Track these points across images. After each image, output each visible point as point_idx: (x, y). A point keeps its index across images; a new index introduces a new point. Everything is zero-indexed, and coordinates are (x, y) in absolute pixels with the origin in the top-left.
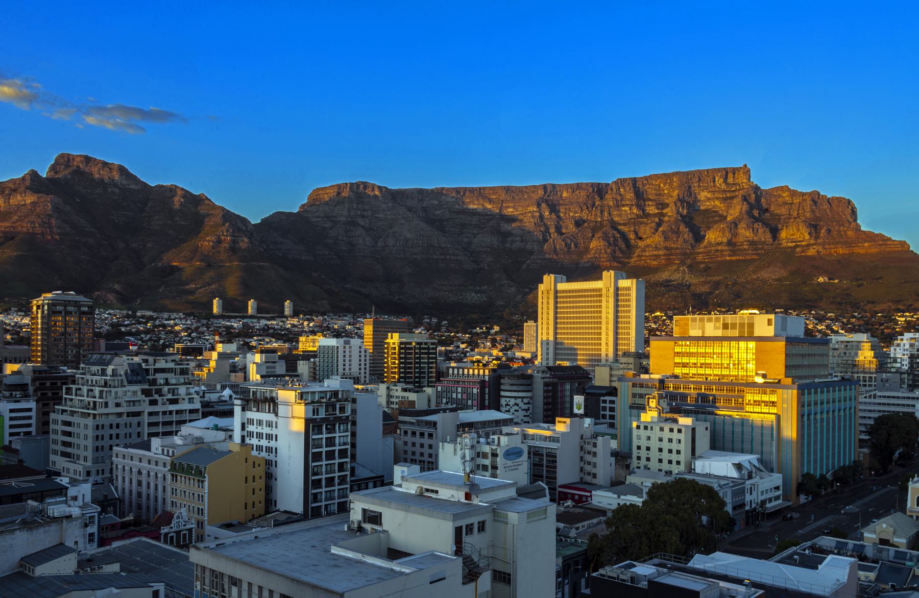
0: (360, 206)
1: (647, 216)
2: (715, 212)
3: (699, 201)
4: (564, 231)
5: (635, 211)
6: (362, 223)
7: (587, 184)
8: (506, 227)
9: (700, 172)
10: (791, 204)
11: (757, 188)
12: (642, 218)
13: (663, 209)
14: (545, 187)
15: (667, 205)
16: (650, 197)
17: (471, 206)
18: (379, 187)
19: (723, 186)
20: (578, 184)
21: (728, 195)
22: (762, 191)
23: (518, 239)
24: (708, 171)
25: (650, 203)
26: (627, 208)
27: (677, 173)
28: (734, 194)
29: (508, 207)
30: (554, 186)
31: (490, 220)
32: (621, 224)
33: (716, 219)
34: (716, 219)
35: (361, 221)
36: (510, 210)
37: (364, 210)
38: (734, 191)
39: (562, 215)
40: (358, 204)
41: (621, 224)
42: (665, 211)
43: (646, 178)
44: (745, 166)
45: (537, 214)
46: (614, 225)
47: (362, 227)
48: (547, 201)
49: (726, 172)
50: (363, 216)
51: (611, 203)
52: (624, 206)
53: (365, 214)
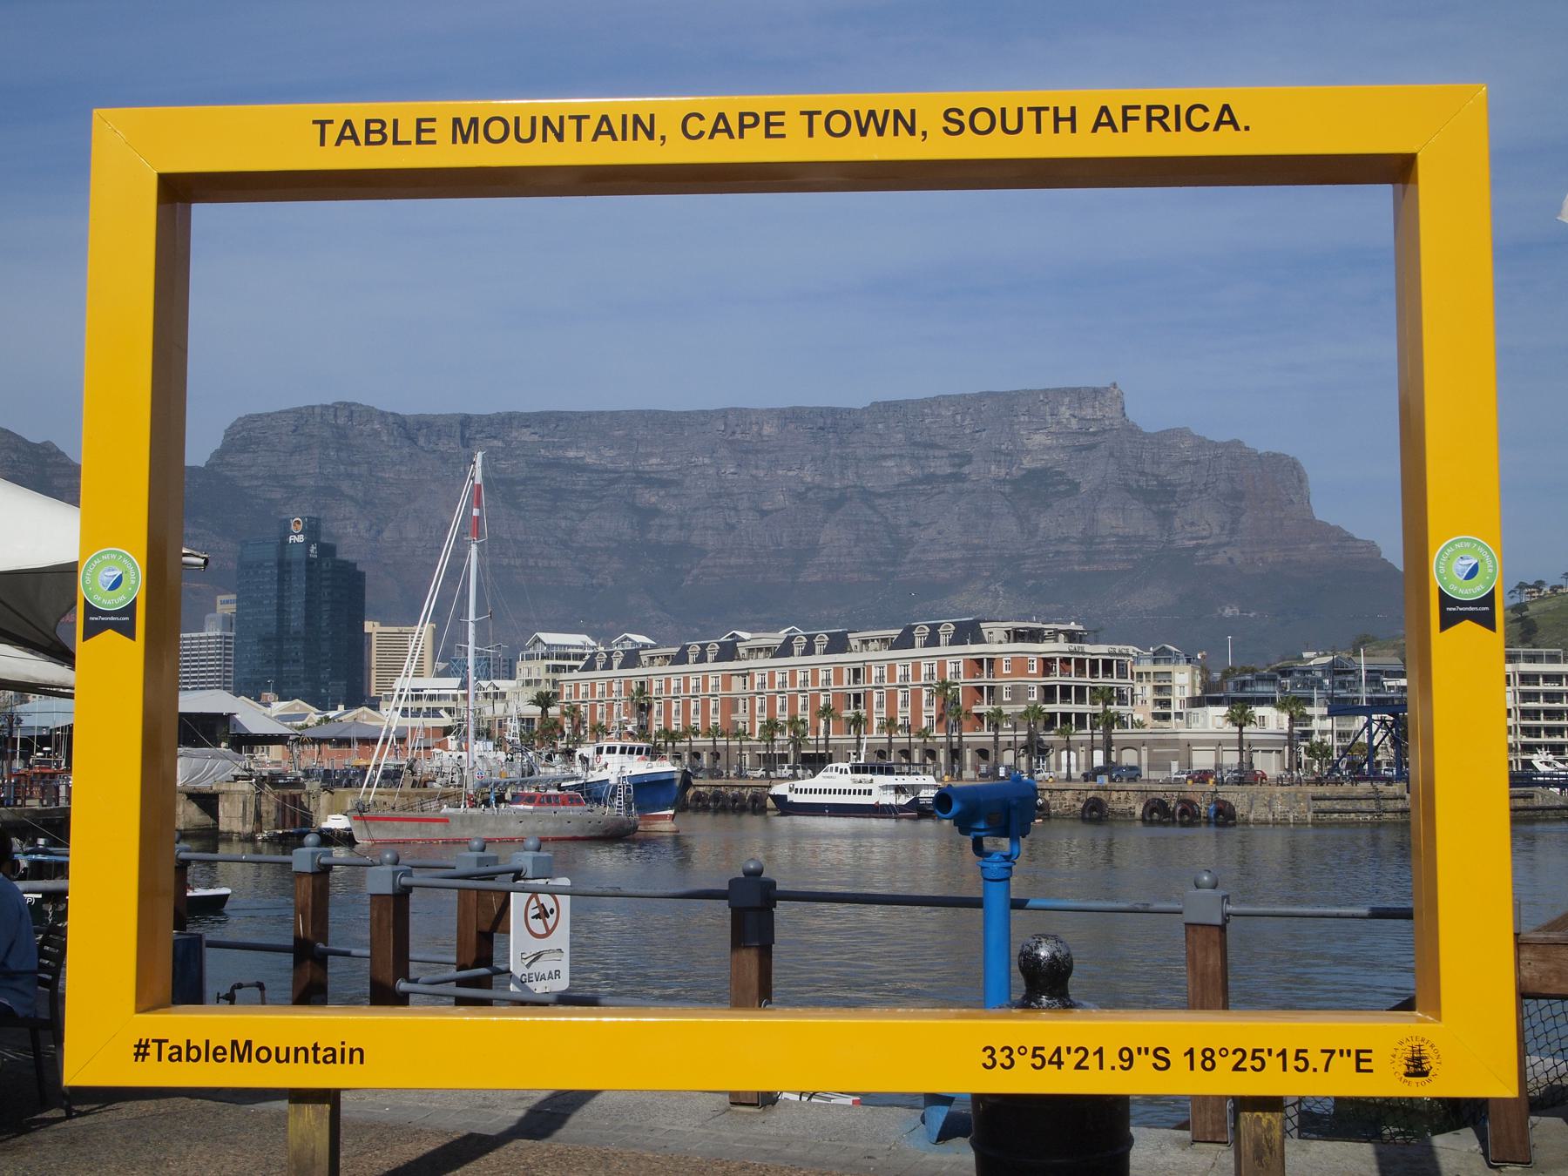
0: (343, 455)
1: (930, 479)
2: (1063, 473)
3: (1029, 452)
4: (767, 506)
5: (907, 469)
6: (351, 492)
7: (811, 410)
8: (649, 497)
9: (1030, 392)
10: (1197, 462)
11: (1133, 430)
12: (921, 482)
13: (961, 466)
14: (724, 414)
15: (967, 459)
16: (938, 440)
17: (571, 454)
18: (383, 414)
19: (1074, 424)
20: (793, 409)
21: (1083, 440)
22: (1146, 436)
23: (673, 522)
24: (1046, 391)
25: (937, 453)
26: (890, 463)
27: (990, 394)
28: (1092, 440)
29: (652, 455)
30: (742, 413)
31: (612, 482)
32: (880, 496)
33: (1062, 488)
34: (1062, 488)
35: (345, 486)
36: (654, 461)
37: (353, 464)
38: (1094, 434)
39: (761, 473)
40: (338, 450)
41: (880, 496)
42: (966, 470)
43: (925, 403)
44: (1115, 385)
45: (711, 471)
46: (867, 496)
47: (352, 498)
48: (731, 443)
49: (1079, 395)
50: (350, 476)
51: (860, 452)
52: (885, 457)
53: (355, 470)
